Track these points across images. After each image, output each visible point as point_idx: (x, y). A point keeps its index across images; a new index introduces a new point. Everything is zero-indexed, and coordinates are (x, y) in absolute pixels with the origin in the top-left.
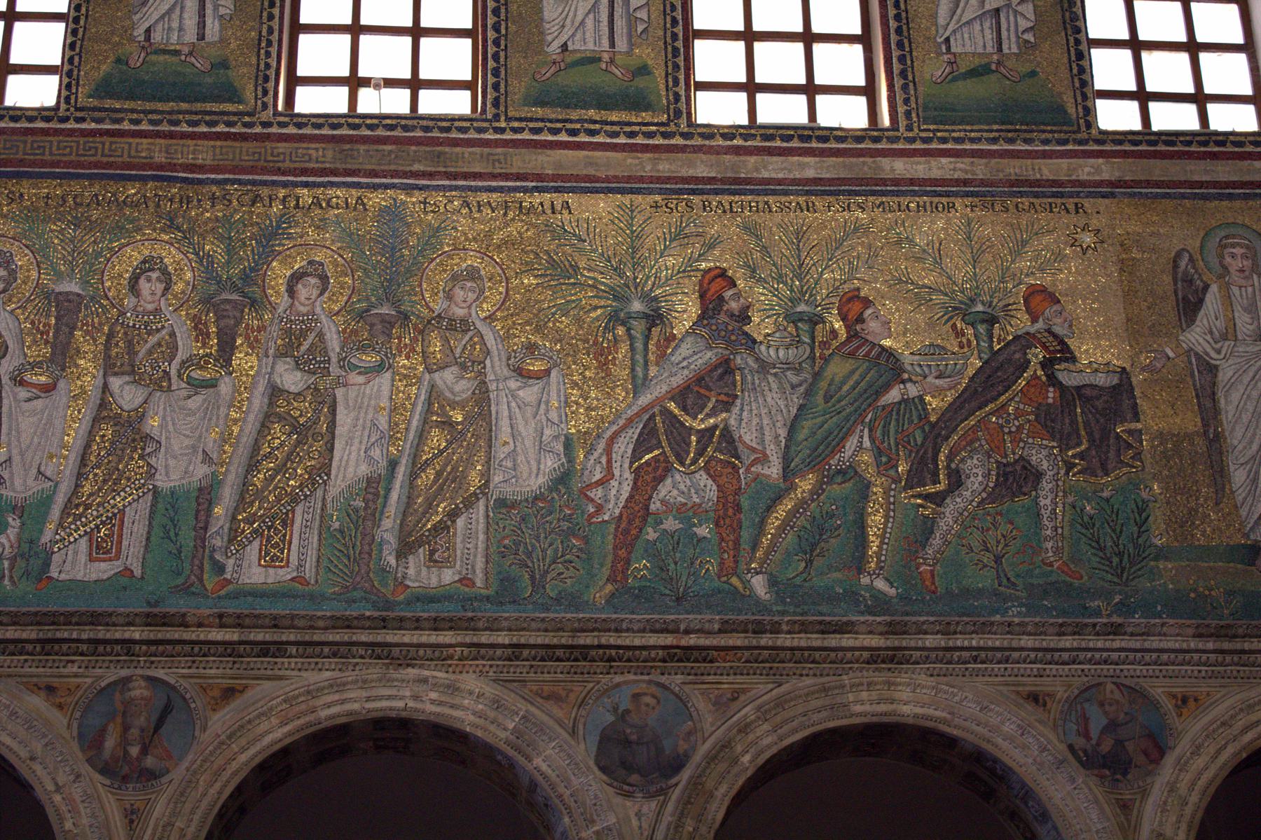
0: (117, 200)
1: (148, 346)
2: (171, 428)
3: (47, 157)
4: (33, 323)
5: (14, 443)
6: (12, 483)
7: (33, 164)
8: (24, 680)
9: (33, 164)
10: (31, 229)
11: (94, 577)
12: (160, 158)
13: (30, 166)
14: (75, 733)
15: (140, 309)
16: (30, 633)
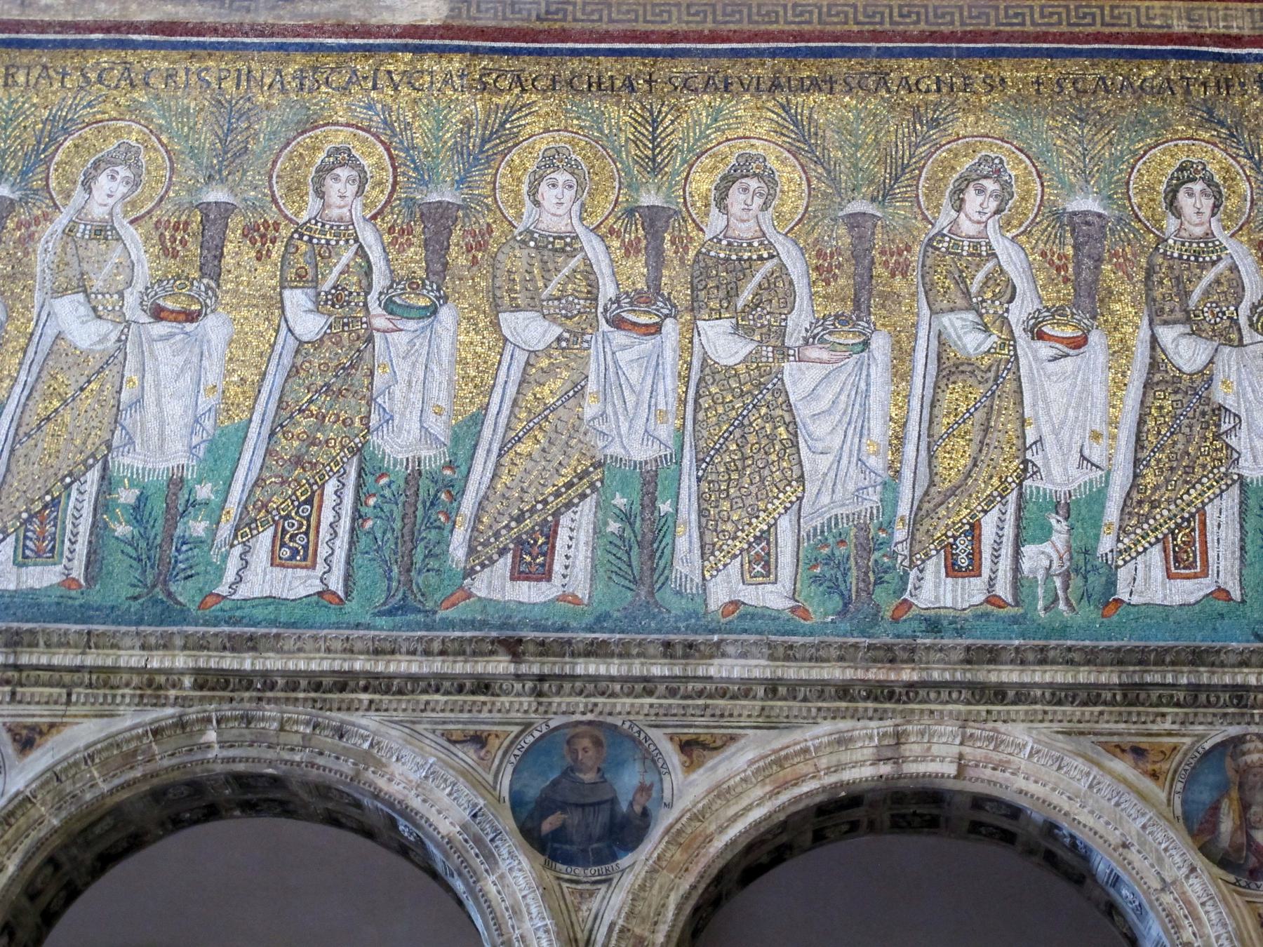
0: (1131, 84)
1: (1204, 283)
2: (1250, 396)
3: (1029, 28)
4: (1043, 254)
5: (1043, 419)
6: (1049, 473)
7: (1010, 37)
8: (1103, 739)
9: (1010, 37)
10: (1022, 126)
11: (1177, 600)
12: (1180, 27)
13: (1007, 41)
14: (1179, 811)
15: (1183, 233)
16: (1110, 676)
